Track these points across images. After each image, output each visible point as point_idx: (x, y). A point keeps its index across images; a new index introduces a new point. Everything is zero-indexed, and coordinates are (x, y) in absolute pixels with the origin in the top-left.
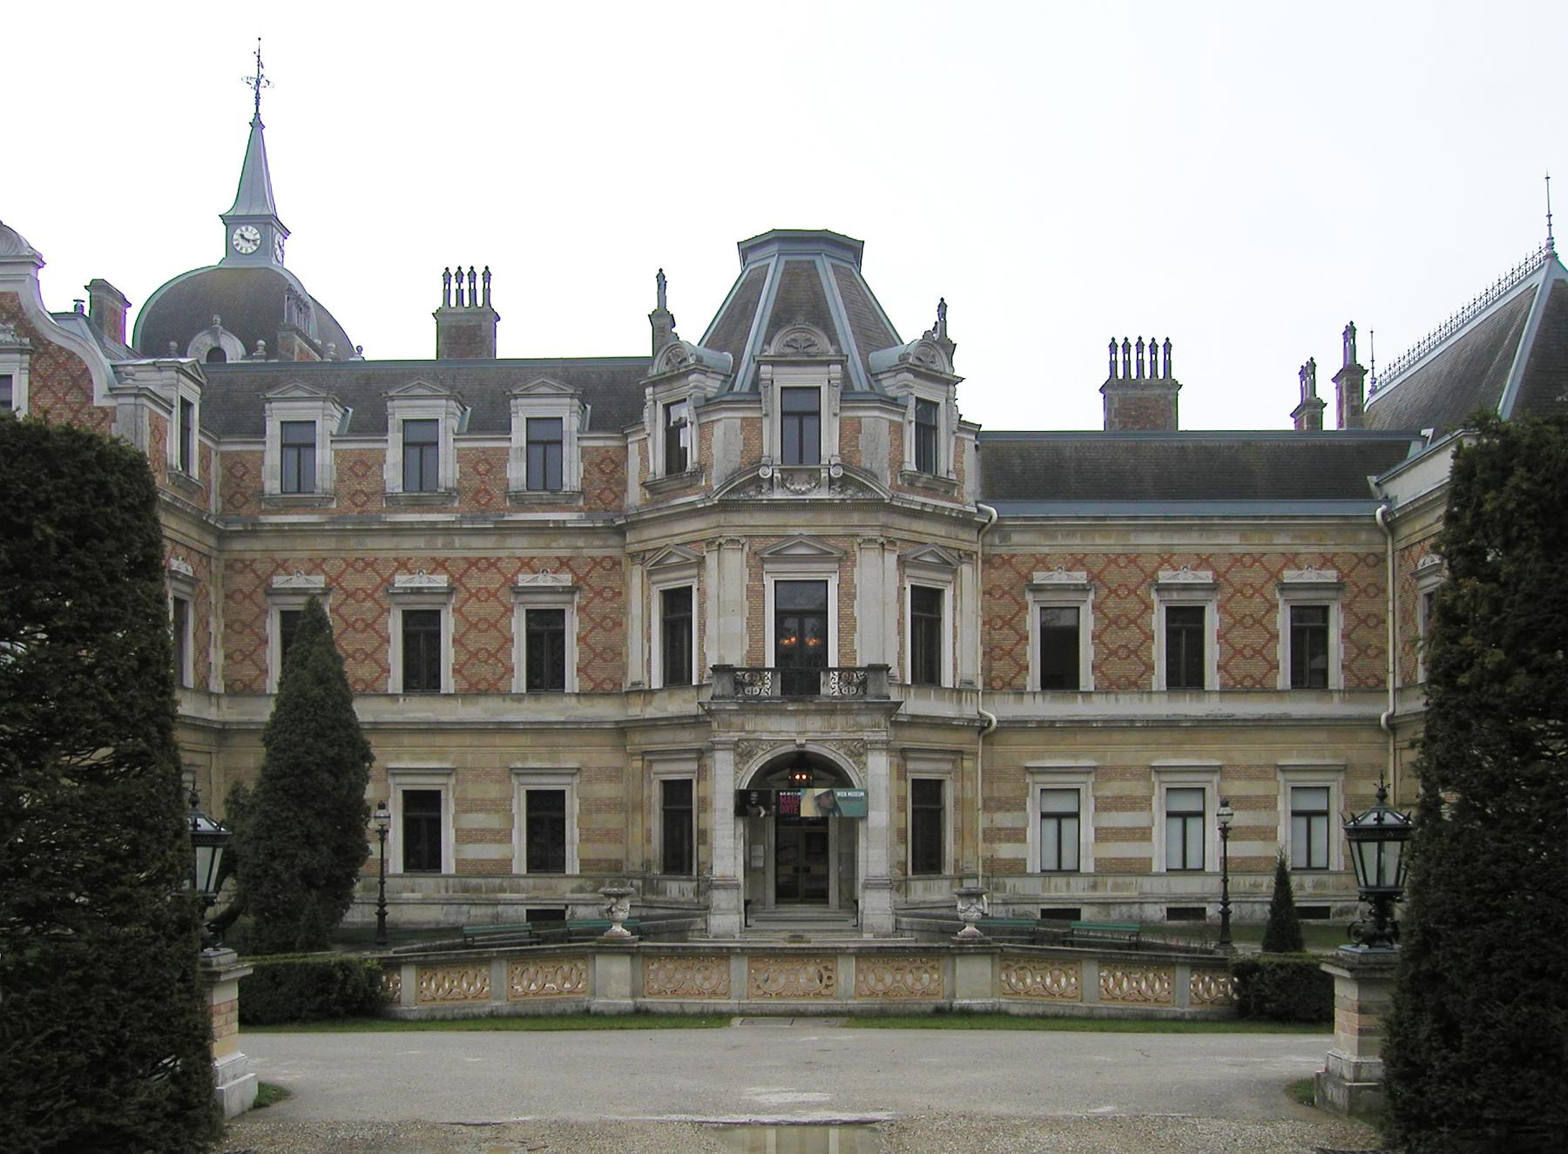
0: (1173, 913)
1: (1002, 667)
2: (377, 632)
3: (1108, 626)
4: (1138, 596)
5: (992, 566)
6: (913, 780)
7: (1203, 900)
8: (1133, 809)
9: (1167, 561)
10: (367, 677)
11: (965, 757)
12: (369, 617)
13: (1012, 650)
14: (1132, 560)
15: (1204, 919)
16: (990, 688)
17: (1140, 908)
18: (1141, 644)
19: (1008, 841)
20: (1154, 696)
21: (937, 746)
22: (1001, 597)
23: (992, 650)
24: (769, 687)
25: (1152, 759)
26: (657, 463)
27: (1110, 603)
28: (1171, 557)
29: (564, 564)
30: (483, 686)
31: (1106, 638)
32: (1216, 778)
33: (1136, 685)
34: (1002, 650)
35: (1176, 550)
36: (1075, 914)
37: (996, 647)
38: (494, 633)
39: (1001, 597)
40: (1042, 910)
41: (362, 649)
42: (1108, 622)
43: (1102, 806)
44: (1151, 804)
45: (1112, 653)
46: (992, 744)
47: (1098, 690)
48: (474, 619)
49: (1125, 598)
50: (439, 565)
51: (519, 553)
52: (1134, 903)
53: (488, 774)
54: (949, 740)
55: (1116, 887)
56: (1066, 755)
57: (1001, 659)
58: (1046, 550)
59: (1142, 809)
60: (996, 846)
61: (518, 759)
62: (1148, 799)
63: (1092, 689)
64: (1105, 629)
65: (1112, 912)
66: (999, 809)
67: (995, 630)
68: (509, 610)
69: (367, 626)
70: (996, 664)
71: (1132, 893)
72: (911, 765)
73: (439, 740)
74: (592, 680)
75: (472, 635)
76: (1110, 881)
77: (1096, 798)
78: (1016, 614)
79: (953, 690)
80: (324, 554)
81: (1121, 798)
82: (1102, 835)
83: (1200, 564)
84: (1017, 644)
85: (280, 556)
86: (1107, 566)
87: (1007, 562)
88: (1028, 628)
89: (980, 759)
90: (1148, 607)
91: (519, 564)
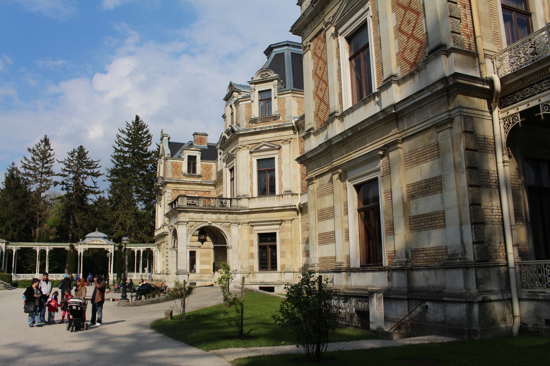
36: (272, 289)
72: (255, 228)
79: (279, 196)
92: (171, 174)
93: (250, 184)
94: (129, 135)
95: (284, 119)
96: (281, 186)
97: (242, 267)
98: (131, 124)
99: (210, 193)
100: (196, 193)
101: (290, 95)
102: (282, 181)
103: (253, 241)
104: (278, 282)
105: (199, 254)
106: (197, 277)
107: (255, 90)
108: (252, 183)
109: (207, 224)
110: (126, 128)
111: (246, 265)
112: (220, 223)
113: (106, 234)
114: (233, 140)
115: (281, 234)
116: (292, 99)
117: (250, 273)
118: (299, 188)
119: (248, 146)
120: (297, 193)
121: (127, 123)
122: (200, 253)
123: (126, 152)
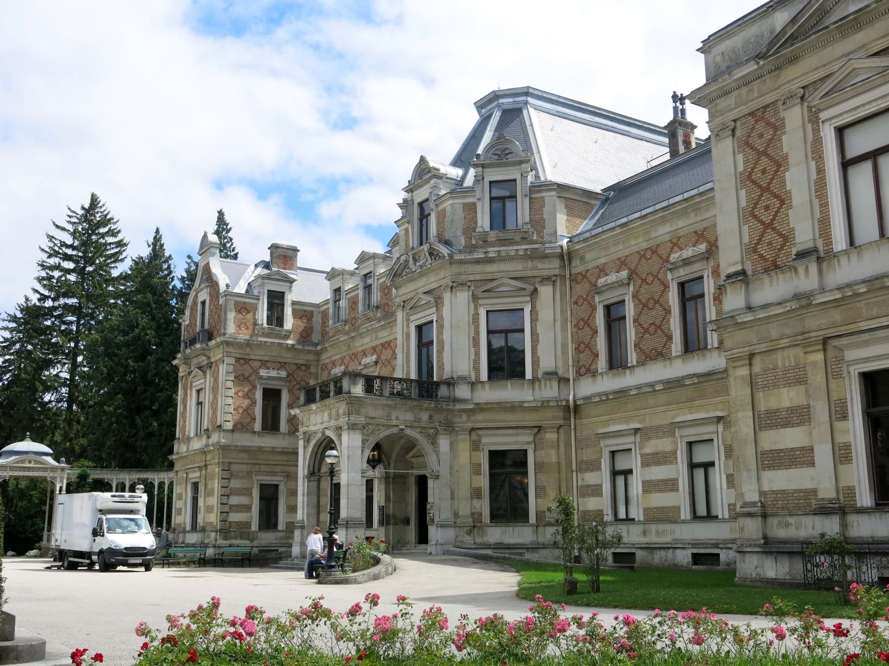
0: (697, 558)
1: (585, 357)
3: (643, 309)
4: (659, 279)
5: (578, 283)
6: (491, 453)
7: (716, 546)
8: (665, 463)
9: (675, 245)
11: (547, 430)
13: (589, 343)
14: (654, 251)
15: (718, 563)
16: (579, 374)
17: (673, 553)
18: (664, 319)
19: (593, 496)
20: (673, 362)
21: (515, 424)
22: (583, 303)
23: (579, 345)
24: (415, 392)
25: (674, 417)
27: (643, 291)
28: (678, 240)
31: (642, 321)
32: (721, 428)
33: (660, 355)
34: (584, 344)
35: (681, 233)
37: (581, 343)
39: (583, 303)
40: (614, 554)
42: (643, 306)
43: (649, 461)
44: (676, 458)
45: (646, 331)
46: (581, 419)
47: (641, 363)
49: (652, 283)
52: (669, 548)
54: (530, 419)
55: (658, 533)
56: (622, 420)
57: (583, 352)
58: (603, 260)
59: (671, 463)
60: (586, 500)
62: (674, 453)
63: (635, 363)
64: (641, 312)
65: (655, 556)
66: (587, 470)
67: (580, 329)
70: (582, 356)
71: (667, 539)
76: (653, 527)
77: (642, 455)
78: (591, 315)
80: (344, 354)
81: (657, 454)
82: (649, 487)
83: (697, 240)
84: (592, 338)
85: (334, 358)
86: (640, 260)
87: (584, 276)
88: (597, 324)
89: (573, 432)
90: (666, 287)
92: (234, 326)
93: (473, 357)
94: (74, 234)
95: (542, 237)
96: (536, 363)
97: (456, 515)
98: (81, 212)
99: (309, 368)
100: (282, 366)
101: (554, 193)
102: (540, 353)
103: (480, 465)
104: (533, 544)
105: (285, 490)
106: (280, 538)
107: (483, 178)
108: (477, 354)
109: (395, 430)
110: (68, 222)
111: (465, 510)
112: (419, 430)
113: (49, 446)
114: (434, 271)
115: (541, 453)
116: (558, 201)
117: (474, 527)
118: (571, 368)
119: (469, 284)
120: (567, 377)
121: (69, 209)
122: (287, 490)
123: (68, 271)
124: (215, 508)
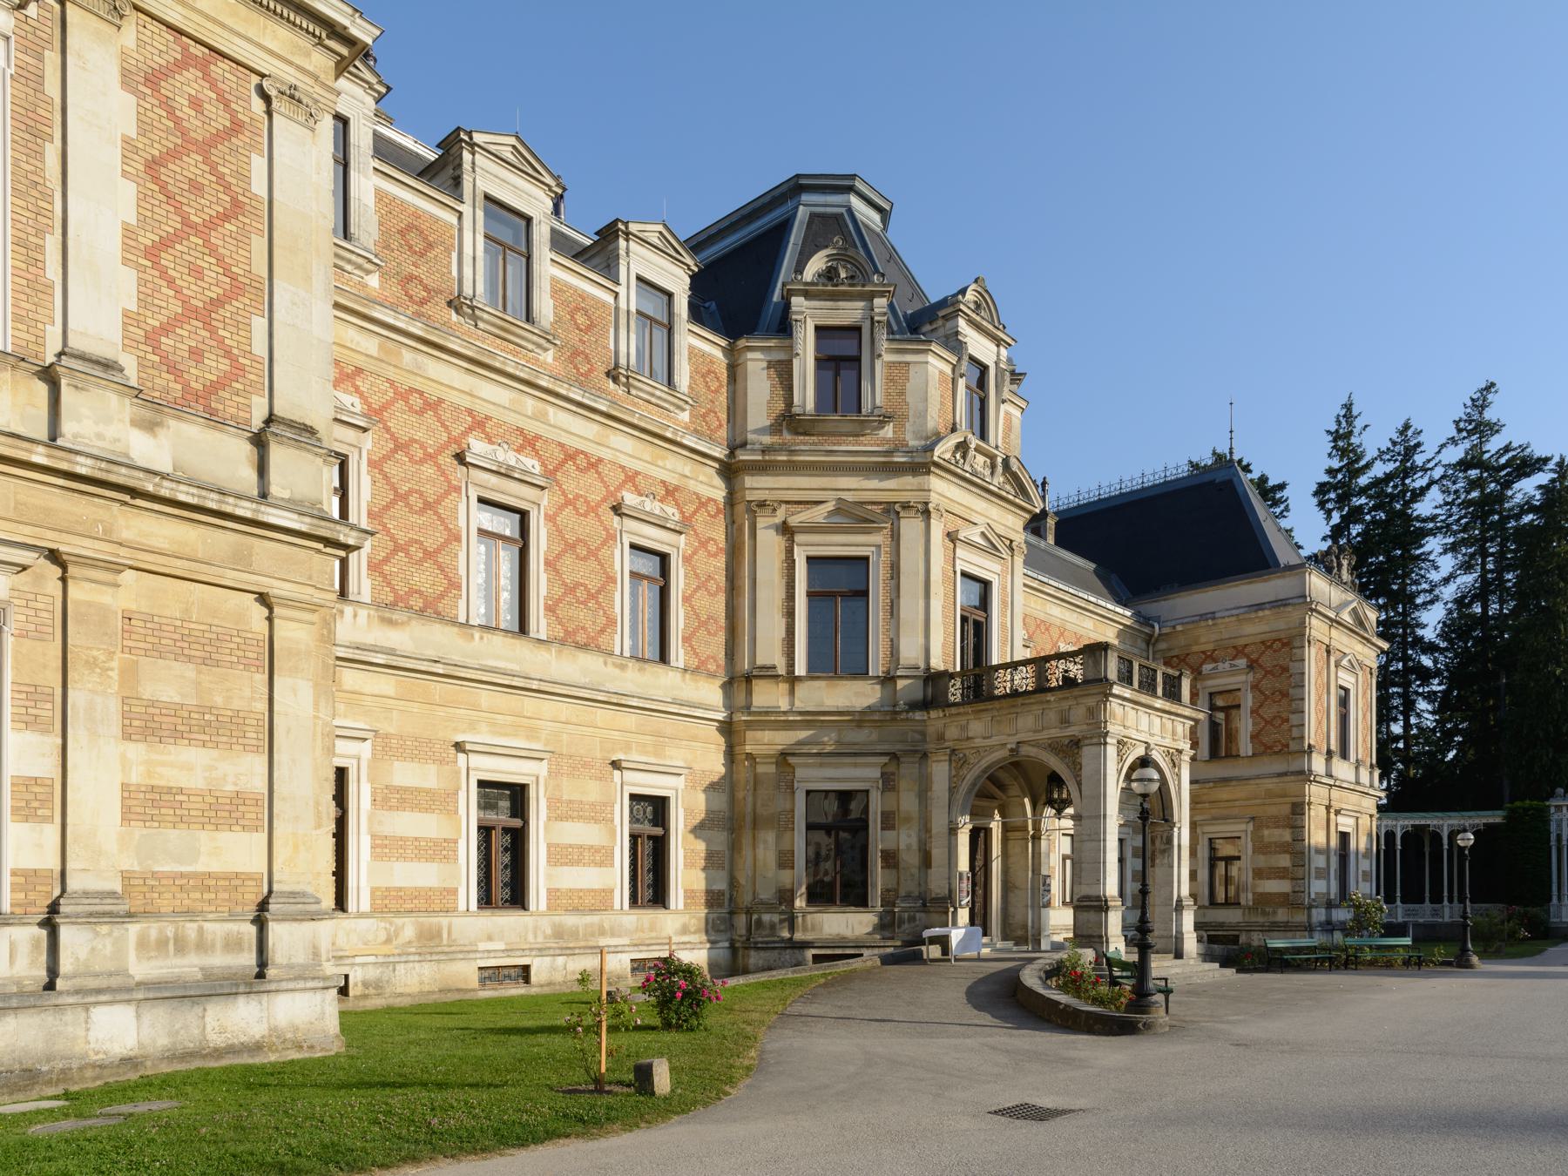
2: (440, 518)
10: (426, 588)
12: (431, 492)
26: (806, 395)
29: (670, 492)
30: (582, 638)
38: (592, 563)
41: (421, 543)
48: (571, 538)
50: (529, 443)
51: (624, 461)
53: (585, 765)
61: (621, 749)
68: (610, 537)
69: (428, 506)
73: (530, 704)
74: (696, 654)
75: (568, 560)
91: (622, 477)
124: (1313, 874)
